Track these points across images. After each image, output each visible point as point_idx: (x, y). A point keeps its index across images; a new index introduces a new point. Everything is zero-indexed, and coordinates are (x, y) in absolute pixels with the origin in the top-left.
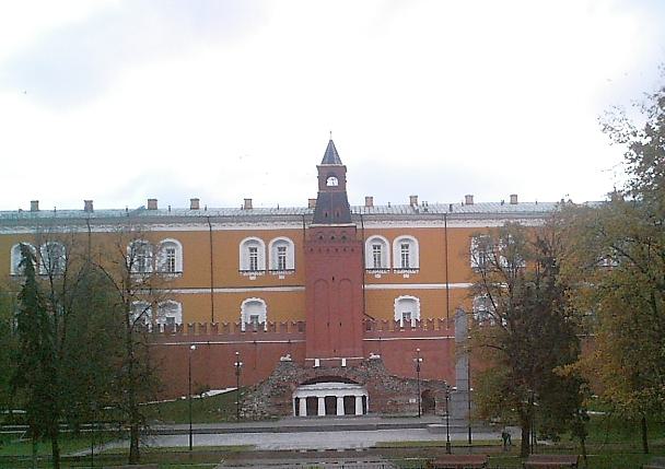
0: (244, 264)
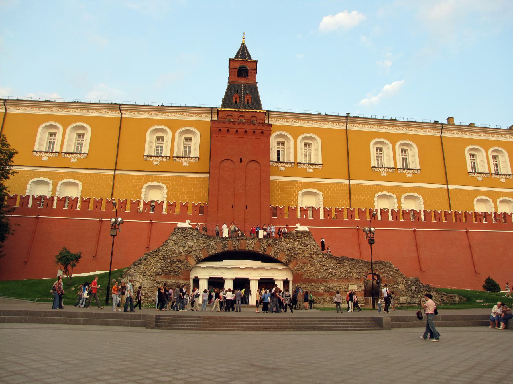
0: (150, 149)
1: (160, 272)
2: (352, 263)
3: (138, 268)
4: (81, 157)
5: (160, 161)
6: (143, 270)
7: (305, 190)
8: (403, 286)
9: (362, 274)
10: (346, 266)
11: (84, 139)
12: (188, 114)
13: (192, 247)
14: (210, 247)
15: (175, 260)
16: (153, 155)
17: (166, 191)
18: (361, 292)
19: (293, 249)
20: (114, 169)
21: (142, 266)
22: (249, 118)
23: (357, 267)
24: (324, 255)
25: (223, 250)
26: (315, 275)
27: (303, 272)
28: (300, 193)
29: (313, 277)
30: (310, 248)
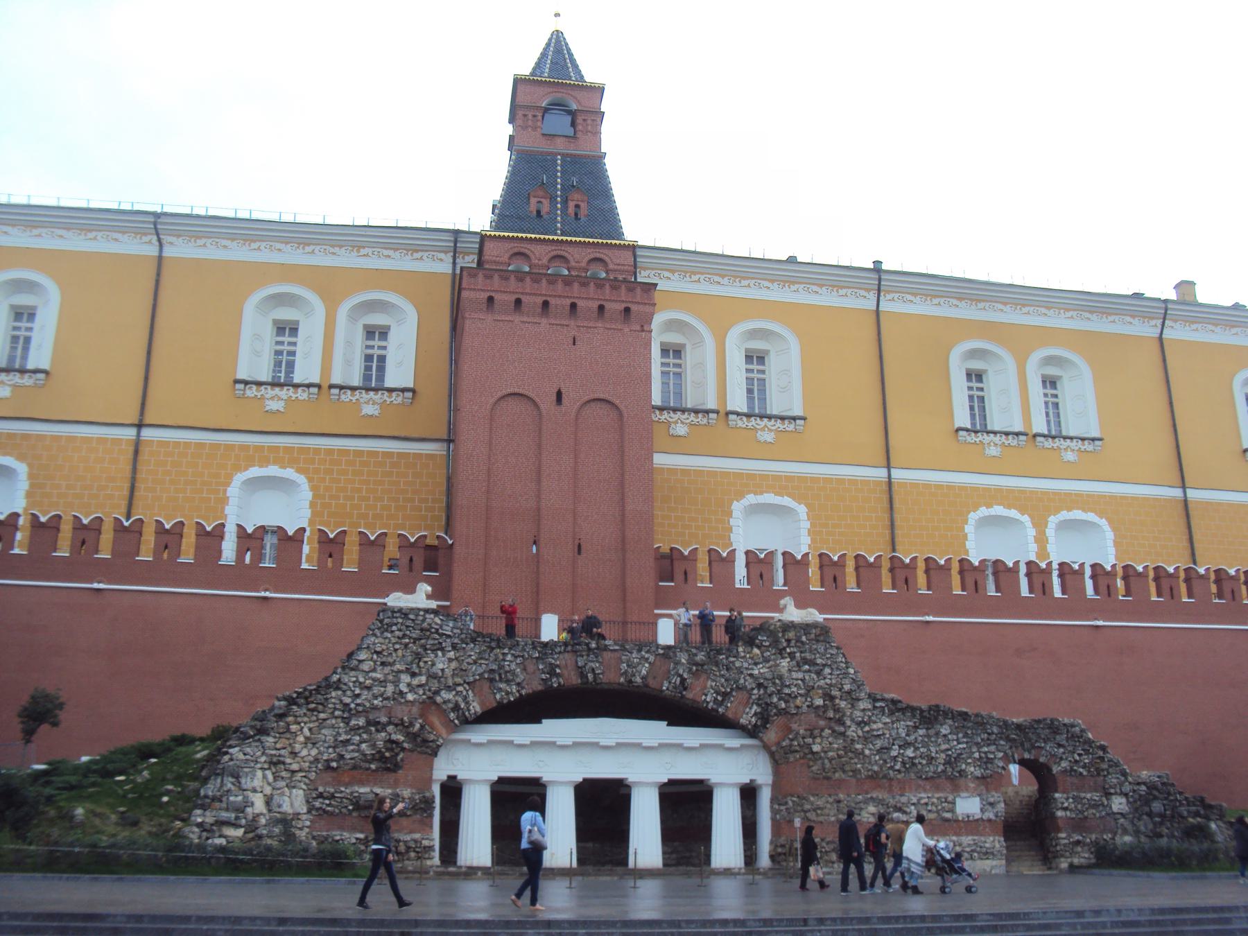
1: (332, 760)
2: (963, 727)
3: (257, 746)
4: (27, 384)
5: (289, 401)
6: (274, 752)
7: (751, 499)
8: (1124, 800)
9: (996, 761)
10: (945, 736)
11: (37, 325)
12: (379, 250)
13: (440, 674)
14: (500, 675)
15: (384, 719)
16: (264, 379)
17: (306, 494)
18: (995, 821)
19: (777, 681)
20: (137, 422)
21: (271, 739)
22: (583, 264)
23: (979, 740)
24: (875, 700)
25: (545, 684)
26: (847, 768)
27: (809, 756)
28: (737, 507)
29: (841, 773)
30: (829, 677)
